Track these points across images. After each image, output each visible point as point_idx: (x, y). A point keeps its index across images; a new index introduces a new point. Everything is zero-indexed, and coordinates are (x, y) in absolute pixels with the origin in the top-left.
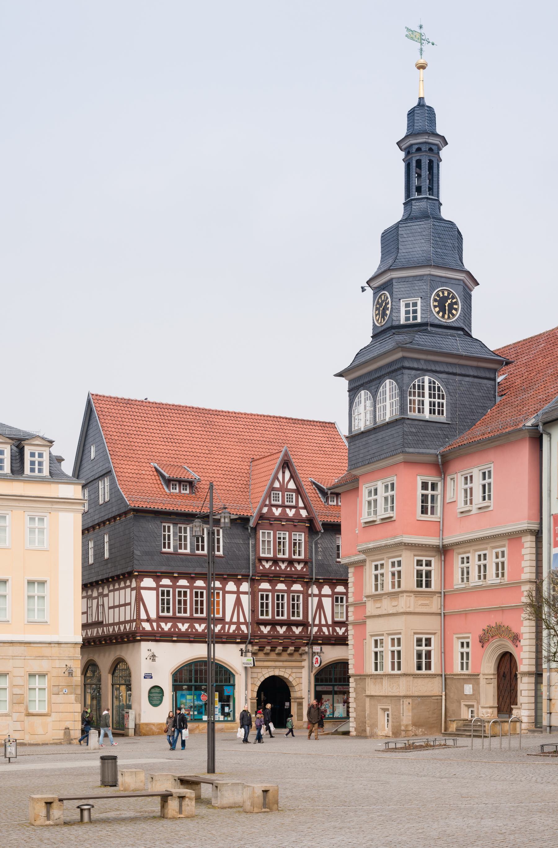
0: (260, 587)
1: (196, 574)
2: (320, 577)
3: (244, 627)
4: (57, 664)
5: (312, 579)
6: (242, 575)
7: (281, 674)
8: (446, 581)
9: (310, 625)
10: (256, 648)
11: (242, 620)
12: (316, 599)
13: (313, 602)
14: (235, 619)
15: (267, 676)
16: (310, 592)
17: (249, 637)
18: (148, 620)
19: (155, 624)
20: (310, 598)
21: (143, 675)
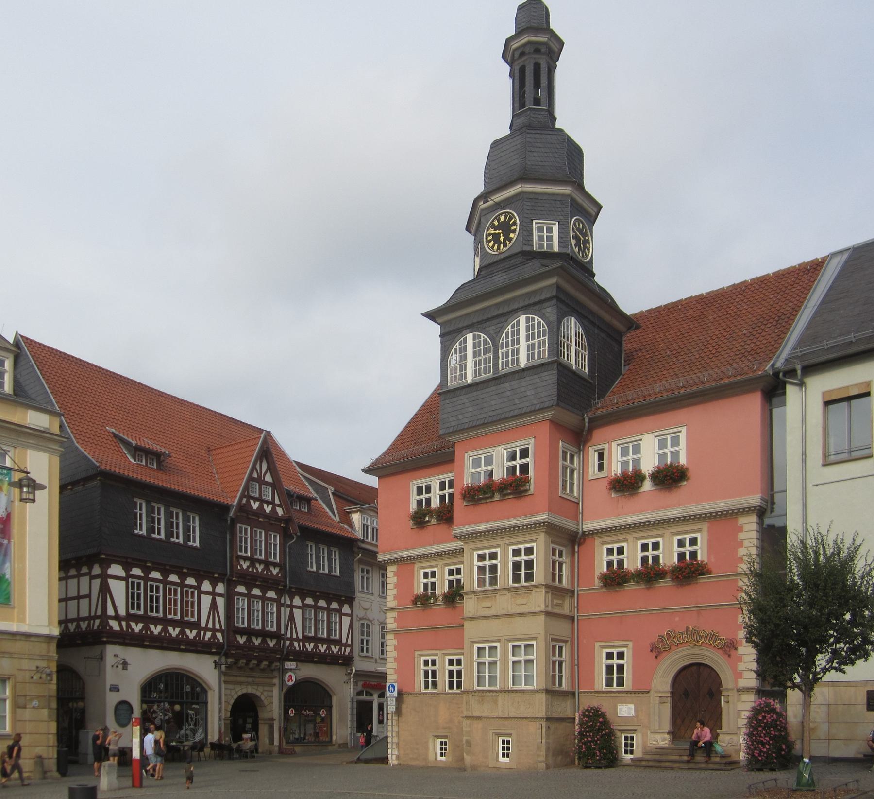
0: (236, 590)
1: (171, 566)
4: (26, 664)
6: (219, 574)
7: (254, 691)
8: (580, 581)
10: (230, 660)
11: (217, 627)
14: (210, 626)
15: (240, 693)
17: (226, 647)
18: (117, 617)
19: (124, 623)
21: (108, 687)
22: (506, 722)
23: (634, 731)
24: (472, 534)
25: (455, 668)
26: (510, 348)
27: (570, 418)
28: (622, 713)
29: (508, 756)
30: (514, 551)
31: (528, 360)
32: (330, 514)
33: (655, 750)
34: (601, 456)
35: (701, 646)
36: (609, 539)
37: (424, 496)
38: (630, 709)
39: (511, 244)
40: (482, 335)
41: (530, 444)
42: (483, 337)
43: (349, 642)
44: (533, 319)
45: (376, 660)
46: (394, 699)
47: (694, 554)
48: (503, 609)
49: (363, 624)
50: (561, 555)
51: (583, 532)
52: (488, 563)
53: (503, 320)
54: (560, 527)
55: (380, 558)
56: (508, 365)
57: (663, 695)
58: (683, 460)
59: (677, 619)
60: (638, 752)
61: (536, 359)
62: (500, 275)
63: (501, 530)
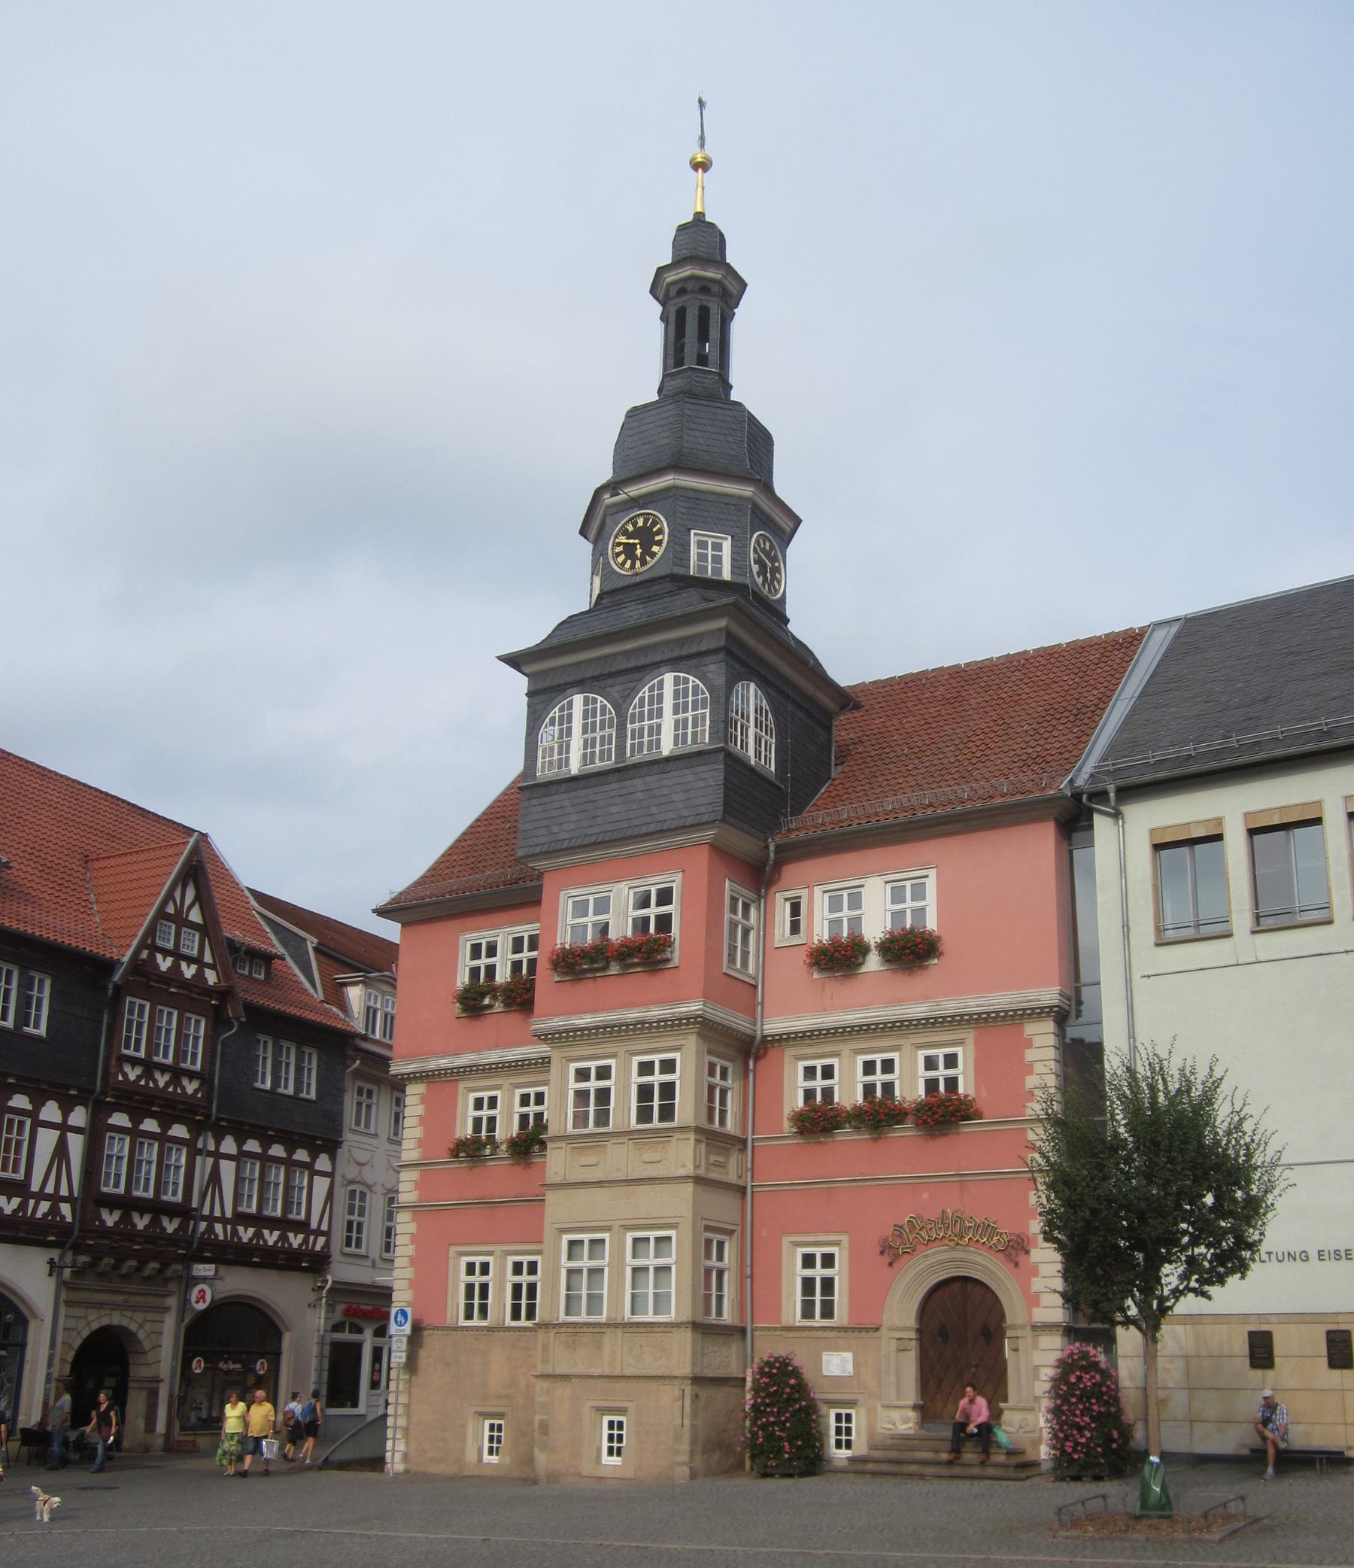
2: (223, 1116)
3: (66, 1209)
5: (208, 1116)
7: (125, 1322)
8: (757, 1119)
9: (194, 1218)
10: (83, 1259)
12: (210, 1161)
13: (203, 1166)
15: (95, 1326)
16: (200, 1145)
20: (199, 1159)
22: (619, 1386)
23: (852, 1404)
24: (567, 1031)
25: (525, 1278)
26: (646, 722)
27: (743, 843)
28: (832, 1369)
29: (619, 1454)
30: (641, 1064)
31: (676, 743)
32: (307, 985)
33: (890, 1442)
34: (796, 909)
35: (967, 1245)
36: (808, 1051)
37: (483, 962)
38: (843, 1360)
39: (654, 561)
40: (600, 698)
41: (676, 882)
42: (601, 702)
43: (324, 1227)
44: (686, 681)
45: (374, 1262)
46: (405, 1339)
47: (952, 1083)
48: (618, 1169)
49: (353, 1193)
50: (724, 1076)
51: (764, 1037)
52: (593, 1084)
53: (636, 678)
54: (724, 1026)
55: (395, 1069)
56: (641, 750)
57: (904, 1335)
58: (931, 924)
59: (925, 1196)
60: (860, 1446)
61: (689, 743)
62: (633, 608)
63: (620, 1026)
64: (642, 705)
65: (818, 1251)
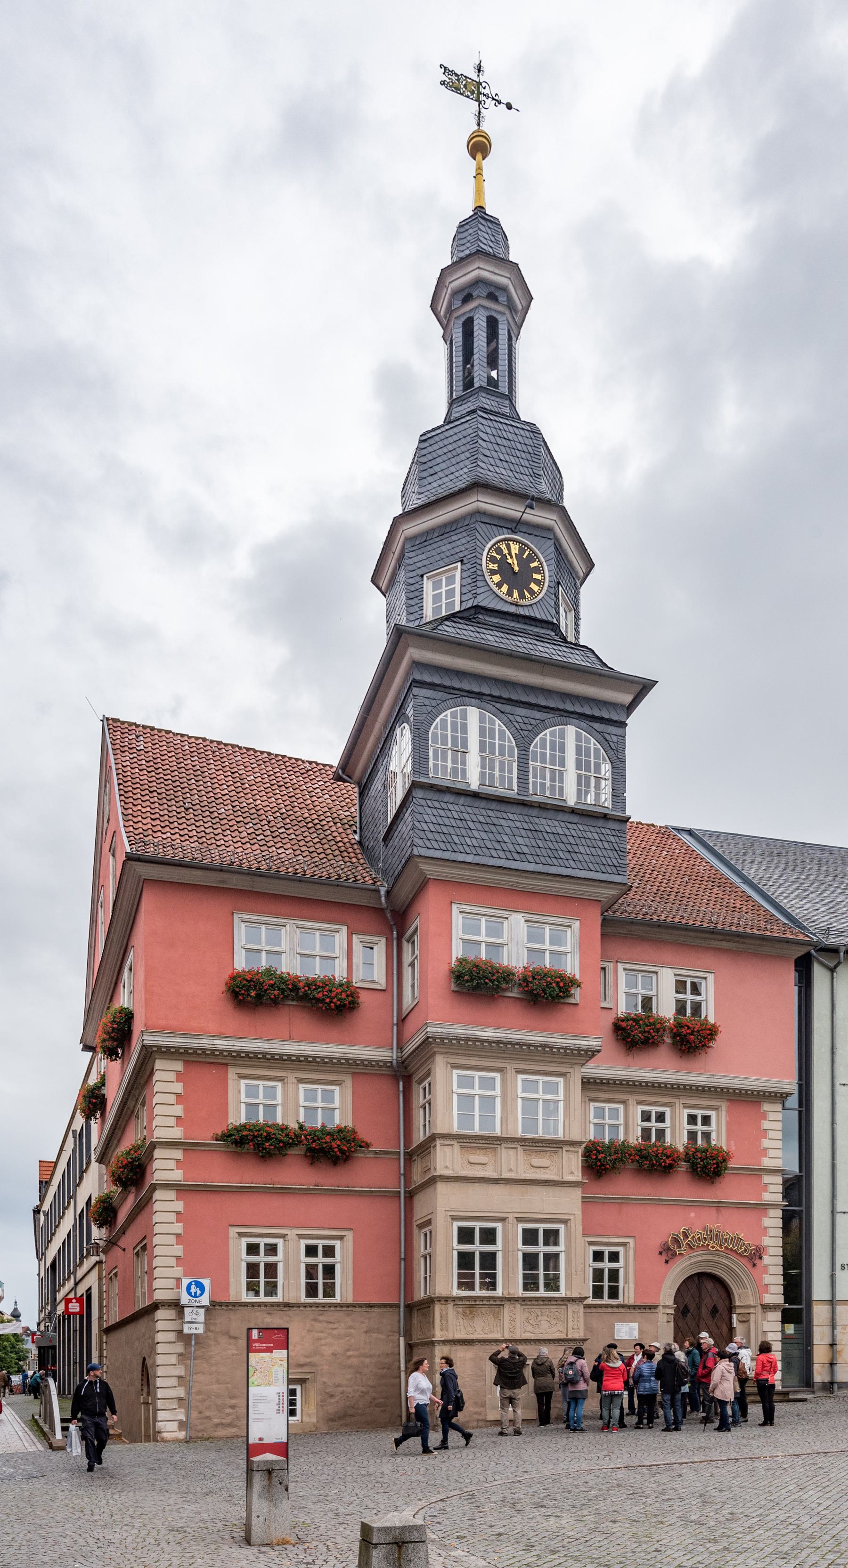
38: (631, 1329)
64: (543, 746)
65: (607, 1250)
